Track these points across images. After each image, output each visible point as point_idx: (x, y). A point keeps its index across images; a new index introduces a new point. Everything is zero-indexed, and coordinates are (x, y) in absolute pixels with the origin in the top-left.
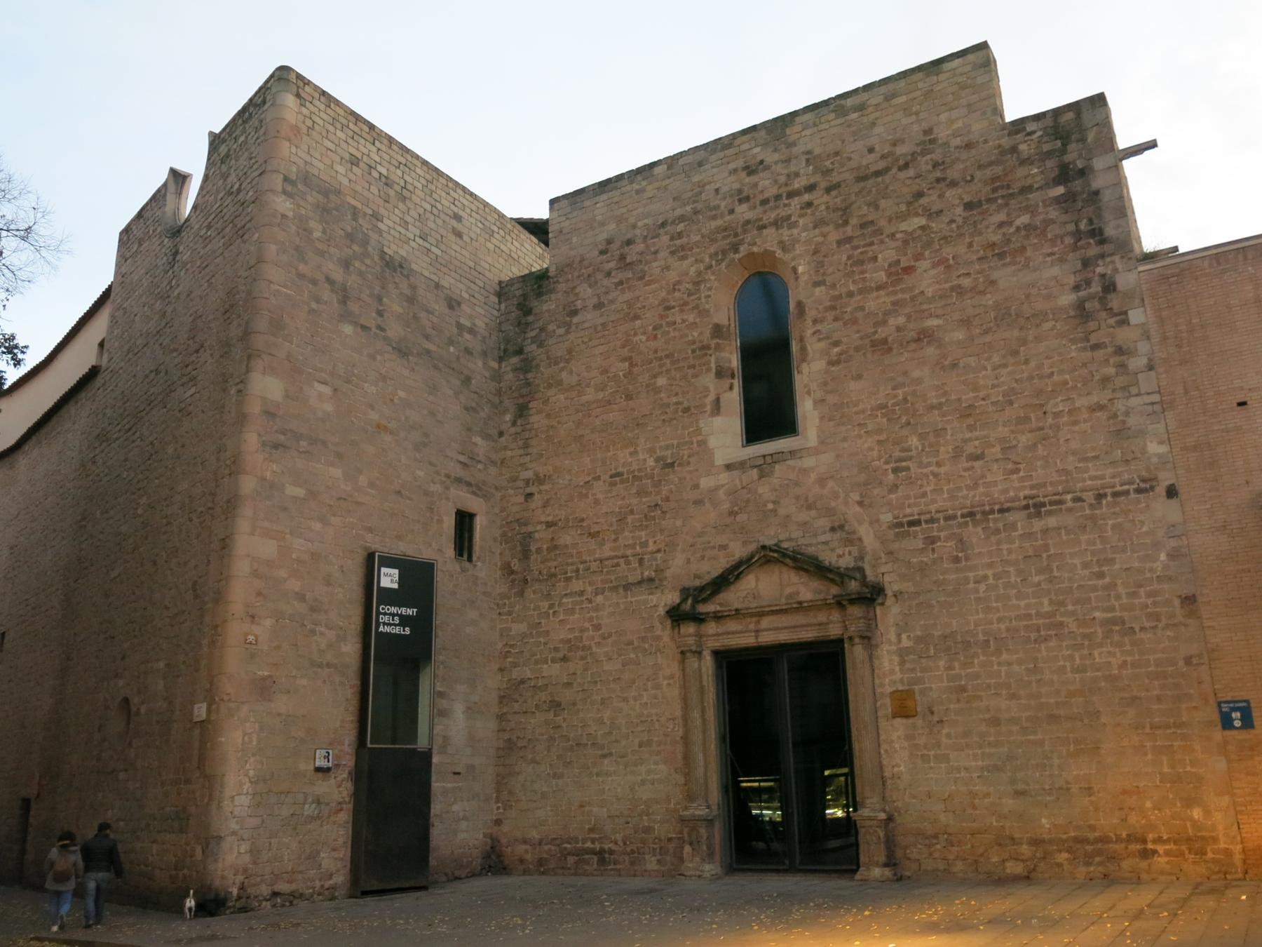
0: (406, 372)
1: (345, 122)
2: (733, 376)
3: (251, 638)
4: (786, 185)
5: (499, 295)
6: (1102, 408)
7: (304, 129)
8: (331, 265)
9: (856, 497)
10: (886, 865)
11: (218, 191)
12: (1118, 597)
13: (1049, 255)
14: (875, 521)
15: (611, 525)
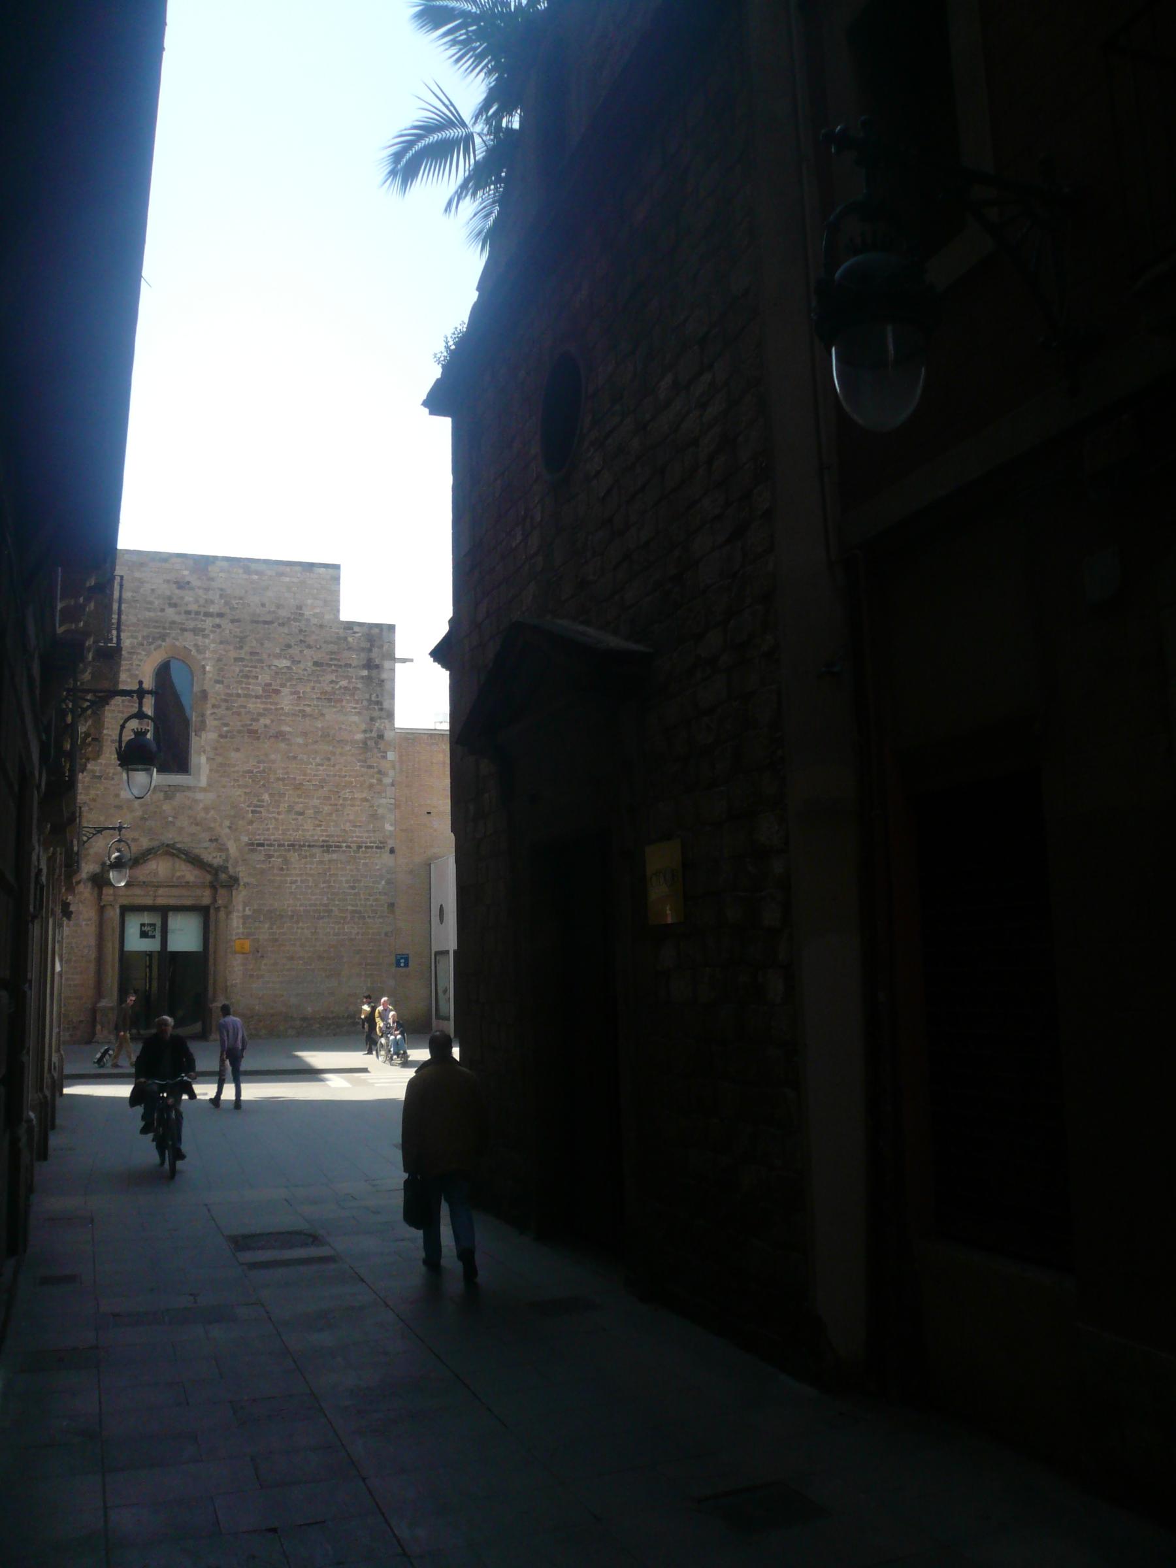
6: (366, 800)
9: (227, 823)
14: (237, 840)
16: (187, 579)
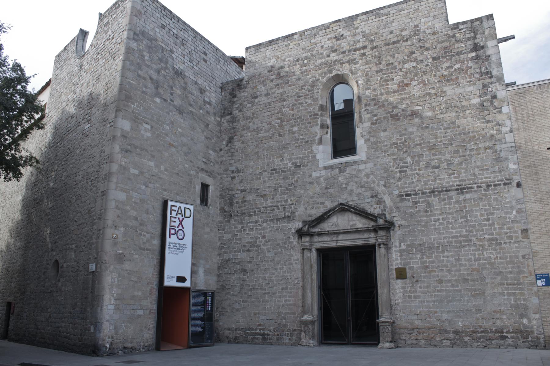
0: (182, 121)
1: (160, 10)
2: (328, 128)
3: (115, 236)
4: (354, 46)
5: (221, 88)
6: (490, 148)
7: (143, 12)
8: (152, 72)
9: (382, 183)
10: (391, 342)
11: (103, 38)
12: (495, 229)
13: (468, 82)
14: (391, 194)
15: (271, 192)
16: (341, 34)
